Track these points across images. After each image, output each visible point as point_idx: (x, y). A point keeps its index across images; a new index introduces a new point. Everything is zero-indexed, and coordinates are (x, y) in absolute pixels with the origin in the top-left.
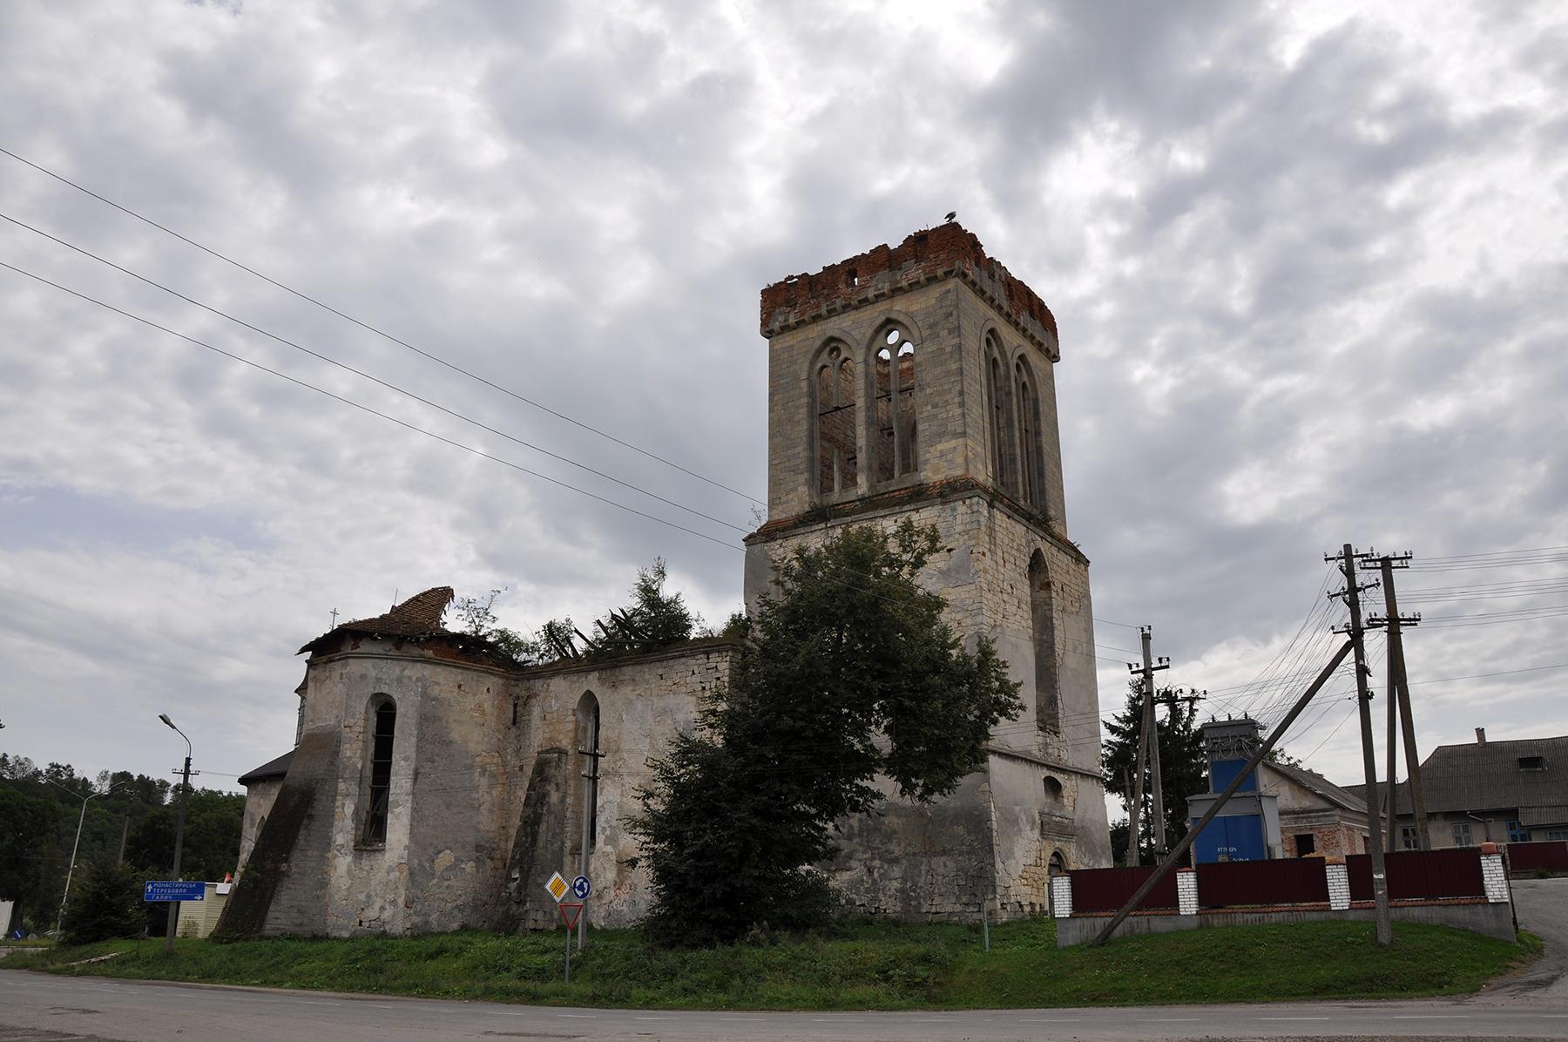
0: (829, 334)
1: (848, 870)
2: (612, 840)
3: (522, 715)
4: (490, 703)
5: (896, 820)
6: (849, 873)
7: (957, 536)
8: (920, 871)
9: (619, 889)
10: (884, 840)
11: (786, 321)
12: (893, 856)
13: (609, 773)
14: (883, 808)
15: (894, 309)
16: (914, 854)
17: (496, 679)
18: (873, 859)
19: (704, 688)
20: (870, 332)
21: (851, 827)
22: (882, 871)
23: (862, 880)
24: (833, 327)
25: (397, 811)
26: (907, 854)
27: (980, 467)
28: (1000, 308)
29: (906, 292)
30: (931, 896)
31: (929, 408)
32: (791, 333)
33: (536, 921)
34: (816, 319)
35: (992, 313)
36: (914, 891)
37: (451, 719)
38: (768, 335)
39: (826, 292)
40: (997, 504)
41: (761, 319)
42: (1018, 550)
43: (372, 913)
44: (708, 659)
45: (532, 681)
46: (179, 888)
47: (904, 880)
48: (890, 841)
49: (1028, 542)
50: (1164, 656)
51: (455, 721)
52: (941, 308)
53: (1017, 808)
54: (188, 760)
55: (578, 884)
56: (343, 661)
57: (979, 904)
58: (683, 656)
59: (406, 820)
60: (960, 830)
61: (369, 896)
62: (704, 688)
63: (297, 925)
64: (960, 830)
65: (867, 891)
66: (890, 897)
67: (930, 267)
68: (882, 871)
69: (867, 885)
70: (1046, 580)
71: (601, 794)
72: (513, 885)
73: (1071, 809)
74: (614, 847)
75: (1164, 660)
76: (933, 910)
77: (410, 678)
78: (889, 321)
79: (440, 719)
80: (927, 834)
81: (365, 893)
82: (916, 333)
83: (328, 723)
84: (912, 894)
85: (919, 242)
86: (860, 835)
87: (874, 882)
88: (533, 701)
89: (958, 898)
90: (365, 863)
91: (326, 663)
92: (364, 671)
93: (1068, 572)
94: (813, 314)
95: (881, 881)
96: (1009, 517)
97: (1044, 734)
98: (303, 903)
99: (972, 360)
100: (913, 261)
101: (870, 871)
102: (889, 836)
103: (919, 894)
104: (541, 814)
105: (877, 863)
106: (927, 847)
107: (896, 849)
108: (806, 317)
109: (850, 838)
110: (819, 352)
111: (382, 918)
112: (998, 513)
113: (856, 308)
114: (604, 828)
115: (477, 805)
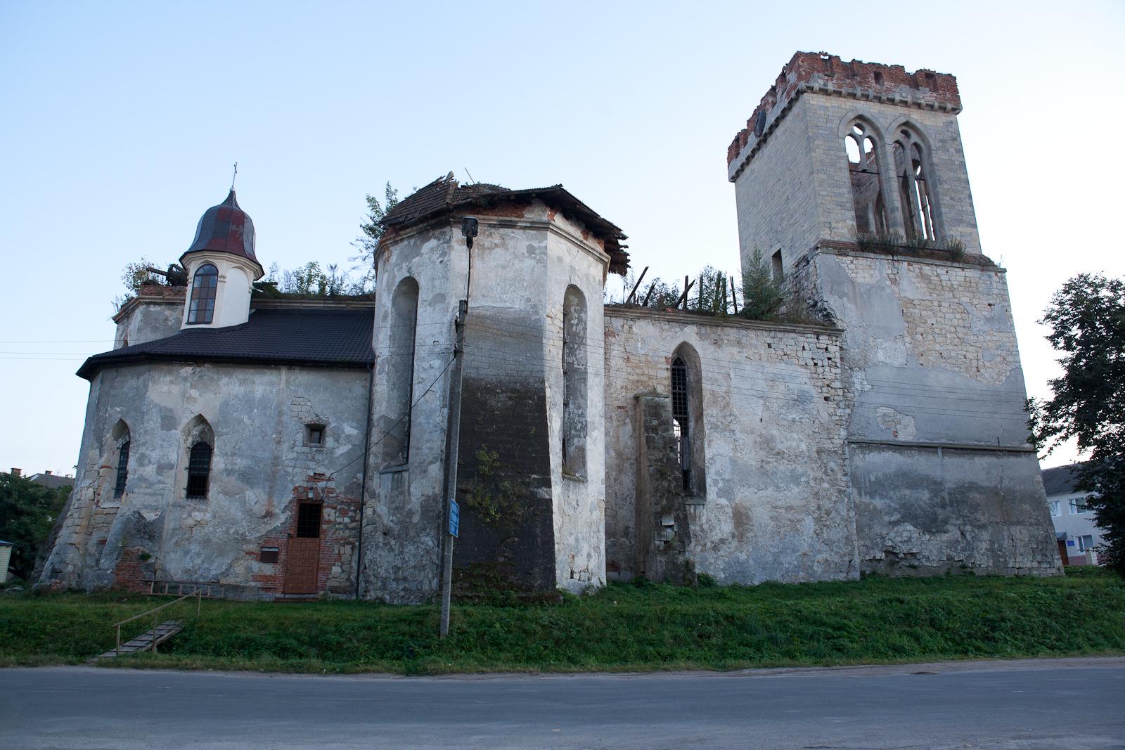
2: (726, 492)
5: (978, 496)
6: (946, 535)
7: (995, 296)
10: (971, 511)
12: (980, 523)
13: (717, 427)
14: (966, 485)
16: (997, 523)
18: (965, 524)
19: (816, 364)
21: (943, 498)
23: (958, 541)
34: (854, 96)
36: (1001, 551)
44: (818, 339)
47: (992, 542)
48: (976, 511)
56: (534, 232)
58: (794, 331)
60: (1027, 507)
61: (577, 540)
64: (1027, 507)
65: (964, 549)
68: (973, 534)
74: (729, 500)
76: (1017, 566)
80: (1004, 508)
83: (508, 305)
85: (928, 78)
87: (968, 543)
91: (494, 226)
95: (974, 542)
102: (975, 508)
103: (1005, 553)
106: (1006, 518)
107: (983, 519)
108: (844, 91)
109: (943, 506)
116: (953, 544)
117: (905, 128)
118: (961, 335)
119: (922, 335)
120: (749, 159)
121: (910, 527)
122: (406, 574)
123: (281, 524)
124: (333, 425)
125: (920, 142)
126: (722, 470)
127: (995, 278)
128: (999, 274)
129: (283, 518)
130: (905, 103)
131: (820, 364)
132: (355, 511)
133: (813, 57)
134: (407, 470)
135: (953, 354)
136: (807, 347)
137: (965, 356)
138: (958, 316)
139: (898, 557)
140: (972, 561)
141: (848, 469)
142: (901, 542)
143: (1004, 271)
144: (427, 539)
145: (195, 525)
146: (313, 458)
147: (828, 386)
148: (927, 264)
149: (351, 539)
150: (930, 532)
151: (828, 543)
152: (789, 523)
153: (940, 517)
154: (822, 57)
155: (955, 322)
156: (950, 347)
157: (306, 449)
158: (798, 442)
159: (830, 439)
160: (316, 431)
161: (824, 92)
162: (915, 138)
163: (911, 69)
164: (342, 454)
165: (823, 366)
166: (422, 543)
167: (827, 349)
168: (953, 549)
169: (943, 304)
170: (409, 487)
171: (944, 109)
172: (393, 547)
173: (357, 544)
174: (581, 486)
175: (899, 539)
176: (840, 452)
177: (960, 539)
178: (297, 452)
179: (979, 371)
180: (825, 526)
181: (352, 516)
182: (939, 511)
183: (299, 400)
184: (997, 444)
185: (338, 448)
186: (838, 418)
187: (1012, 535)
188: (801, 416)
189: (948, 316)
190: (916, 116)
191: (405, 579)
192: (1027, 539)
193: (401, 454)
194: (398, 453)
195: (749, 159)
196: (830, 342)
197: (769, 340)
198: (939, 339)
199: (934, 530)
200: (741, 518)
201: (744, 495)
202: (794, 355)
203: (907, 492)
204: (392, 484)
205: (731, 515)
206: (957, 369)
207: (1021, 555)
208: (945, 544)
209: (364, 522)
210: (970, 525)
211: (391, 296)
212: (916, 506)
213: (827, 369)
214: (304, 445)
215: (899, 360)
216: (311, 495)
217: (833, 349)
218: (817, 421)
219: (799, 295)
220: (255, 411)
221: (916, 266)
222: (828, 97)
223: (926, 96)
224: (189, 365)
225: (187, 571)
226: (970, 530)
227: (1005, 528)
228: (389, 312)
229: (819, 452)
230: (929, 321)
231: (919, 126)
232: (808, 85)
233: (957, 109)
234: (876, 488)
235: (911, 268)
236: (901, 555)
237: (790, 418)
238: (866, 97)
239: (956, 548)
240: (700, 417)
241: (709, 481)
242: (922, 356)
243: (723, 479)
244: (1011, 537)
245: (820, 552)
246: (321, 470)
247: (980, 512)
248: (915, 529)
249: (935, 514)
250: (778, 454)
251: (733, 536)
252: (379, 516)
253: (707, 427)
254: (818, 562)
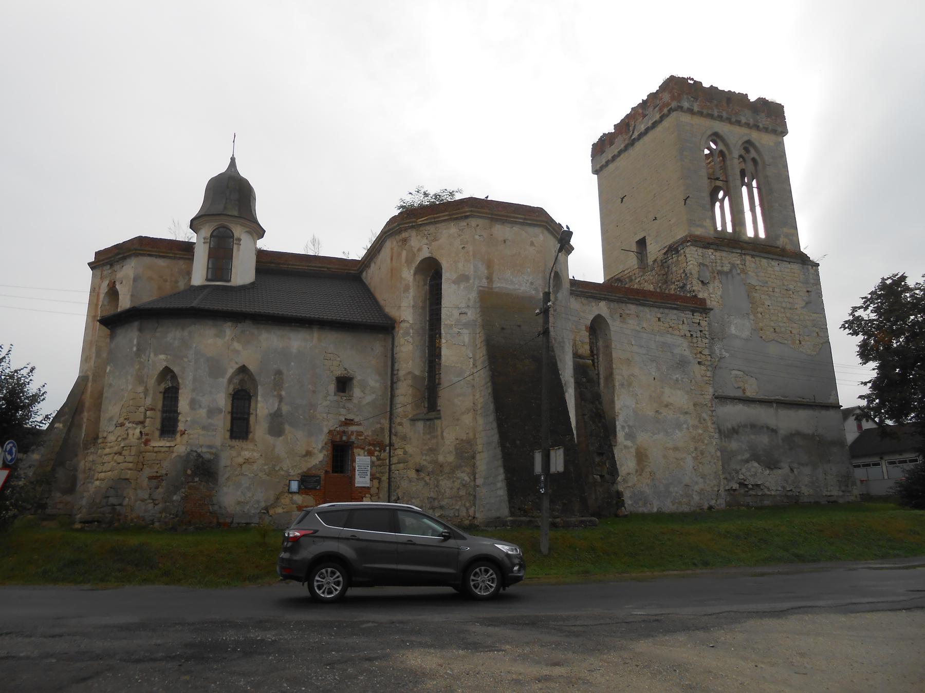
0: (716, 130)
2: (630, 436)
6: (780, 470)
9: (641, 475)
19: (692, 335)
22: (799, 470)
34: (711, 116)
44: (693, 315)
62: (692, 335)
71: (618, 399)
85: (763, 104)
101: (792, 470)
108: (705, 112)
114: (623, 427)
117: (747, 146)
118: (788, 315)
119: (761, 314)
120: (614, 158)
121: (756, 464)
122: (443, 503)
123: (320, 462)
124: (359, 378)
125: (757, 157)
126: (627, 418)
127: (812, 271)
128: (814, 268)
129: (320, 457)
130: (747, 125)
131: (694, 336)
132: (380, 451)
133: (683, 81)
134: (440, 418)
135: (783, 329)
136: (685, 322)
137: (791, 331)
138: (786, 300)
139: (747, 488)
141: (715, 419)
142: (750, 476)
143: (818, 265)
144: (463, 475)
145: (244, 463)
146: (344, 406)
147: (700, 353)
148: (765, 258)
149: (378, 475)
150: (769, 468)
151: (703, 477)
152: (675, 460)
154: (689, 81)
155: (784, 305)
156: (781, 325)
157: (336, 398)
158: (679, 398)
159: (702, 395)
160: (344, 384)
161: (691, 111)
162: (753, 154)
163: (752, 98)
164: (367, 404)
165: (697, 337)
166: (458, 478)
167: (699, 323)
169: (776, 290)
170: (442, 432)
171: (774, 132)
172: (428, 481)
173: (385, 478)
175: (748, 473)
176: (710, 405)
178: (329, 400)
179: (800, 343)
180: (700, 463)
181: (377, 456)
183: (330, 355)
184: (813, 401)
185: (364, 398)
186: (707, 378)
188: (683, 376)
189: (780, 299)
190: (755, 136)
191: (442, 507)
193: (423, 404)
194: (421, 404)
195: (614, 158)
196: (701, 318)
197: (659, 315)
198: (774, 318)
199: (772, 467)
200: (641, 457)
201: (642, 438)
202: (677, 328)
203: (753, 437)
204: (424, 430)
205: (635, 454)
206: (786, 342)
209: (394, 460)
211: (412, 272)
213: (700, 339)
214: (335, 395)
215: (746, 333)
216: (344, 438)
217: (703, 323)
218: (693, 381)
219: (667, 278)
220: (293, 364)
221: (757, 259)
223: (763, 120)
224: (230, 321)
225: (239, 503)
228: (411, 284)
229: (695, 405)
230: (767, 303)
231: (757, 144)
232: (679, 104)
233: (784, 132)
234: (734, 432)
235: (753, 259)
236: (750, 486)
237: (674, 377)
238: (720, 118)
240: (610, 377)
241: (618, 427)
242: (762, 330)
243: (629, 426)
245: (697, 483)
246: (350, 417)
250: (667, 406)
251: (637, 471)
252: (411, 456)
253: (617, 384)
254: (696, 491)
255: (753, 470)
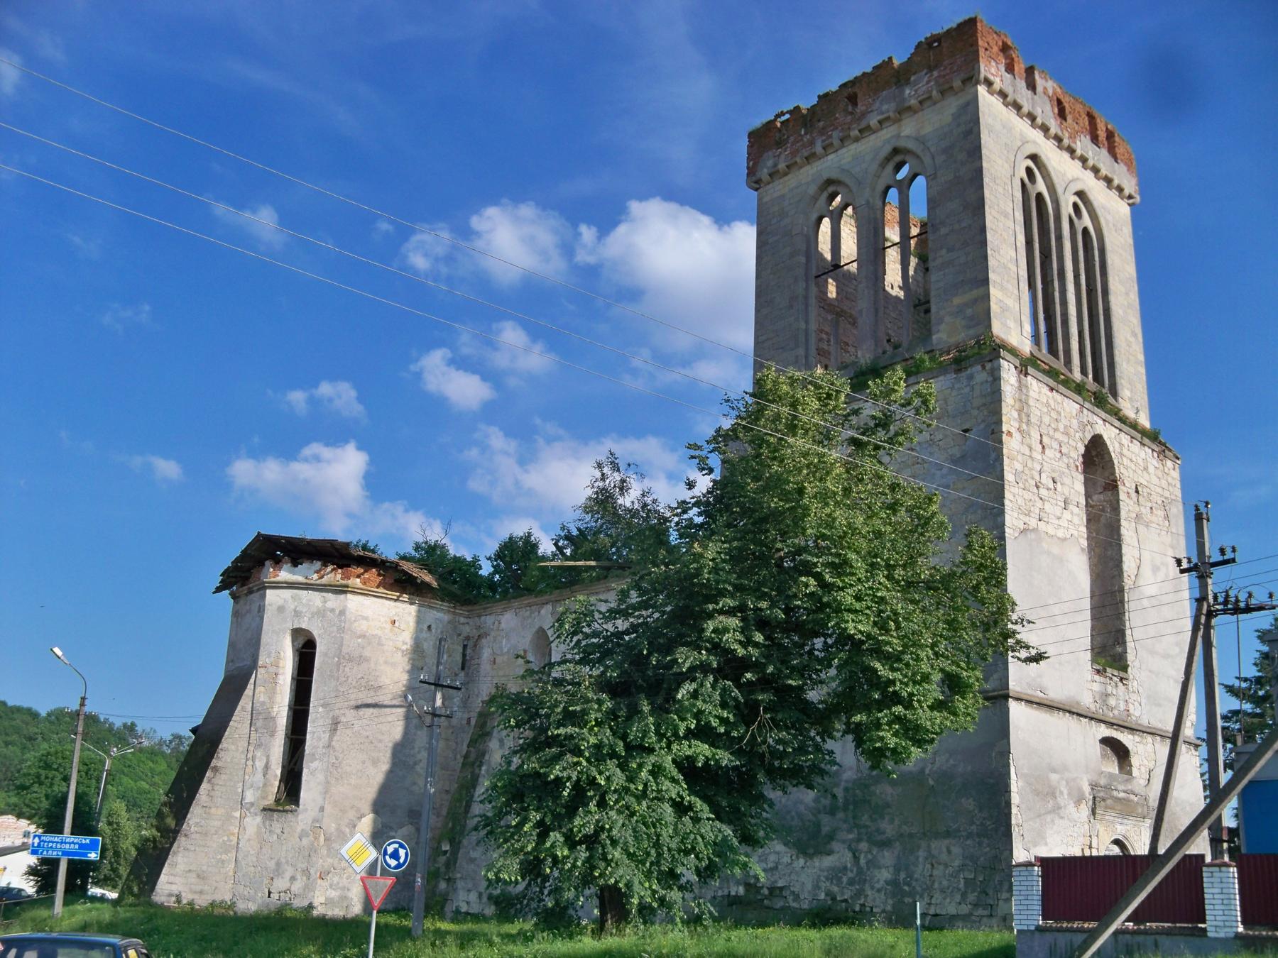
0: (825, 176)
1: (829, 855)
3: (472, 658)
4: (431, 643)
6: (830, 858)
7: (975, 412)
8: (917, 858)
10: (874, 816)
11: (775, 165)
12: (883, 837)
15: (902, 134)
16: (911, 835)
17: (440, 615)
18: (859, 840)
20: (875, 166)
23: (845, 868)
24: (829, 165)
25: (316, 764)
26: (902, 835)
27: (1011, 324)
28: (1045, 129)
29: (915, 112)
30: (928, 889)
31: (944, 251)
32: (781, 181)
33: (468, 903)
34: (810, 158)
35: (1037, 135)
36: (909, 885)
37: (381, 660)
38: (758, 186)
39: (821, 124)
40: (1030, 370)
41: (748, 168)
42: (1066, 433)
43: (281, 884)
45: (483, 618)
46: (70, 843)
47: (897, 869)
49: (1083, 426)
50: (1227, 544)
51: (386, 662)
52: (959, 125)
53: (1054, 777)
54: (83, 699)
55: (390, 850)
57: (991, 906)
59: (321, 777)
60: (969, 804)
61: (278, 864)
63: (195, 892)
66: (879, 891)
67: (944, 76)
68: (870, 856)
69: (850, 875)
70: (1112, 478)
72: (442, 859)
73: (1143, 782)
75: (1228, 551)
76: (932, 911)
77: (332, 610)
78: (896, 151)
79: (367, 660)
81: (276, 860)
82: (927, 160)
83: (245, 663)
84: (906, 888)
86: (845, 809)
87: (860, 871)
88: (484, 641)
89: (964, 895)
90: (277, 827)
91: (246, 595)
92: (281, 602)
93: (1146, 469)
94: (806, 154)
95: (868, 869)
96: (1052, 389)
97: (1102, 679)
98: (204, 868)
99: (1001, 190)
100: (925, 71)
102: (880, 810)
104: (478, 776)
105: (864, 846)
109: (832, 812)
110: (815, 199)
111: (292, 889)
112: (1034, 382)
113: (857, 140)
115: (411, 763)
116: (835, 875)
121: (779, 847)
140: (862, 902)
153: (825, 830)
168: (834, 882)
174: (290, 815)
177: (849, 865)
182: (825, 819)
187: (933, 857)
192: (957, 863)
207: (942, 891)
208: (826, 874)
210: (868, 841)
212: (793, 813)
222: (786, 178)
226: (865, 849)
227: (923, 844)
239: (839, 879)
244: (929, 860)
247: (887, 817)
248: (788, 850)
249: (818, 825)
255: (772, 858)
